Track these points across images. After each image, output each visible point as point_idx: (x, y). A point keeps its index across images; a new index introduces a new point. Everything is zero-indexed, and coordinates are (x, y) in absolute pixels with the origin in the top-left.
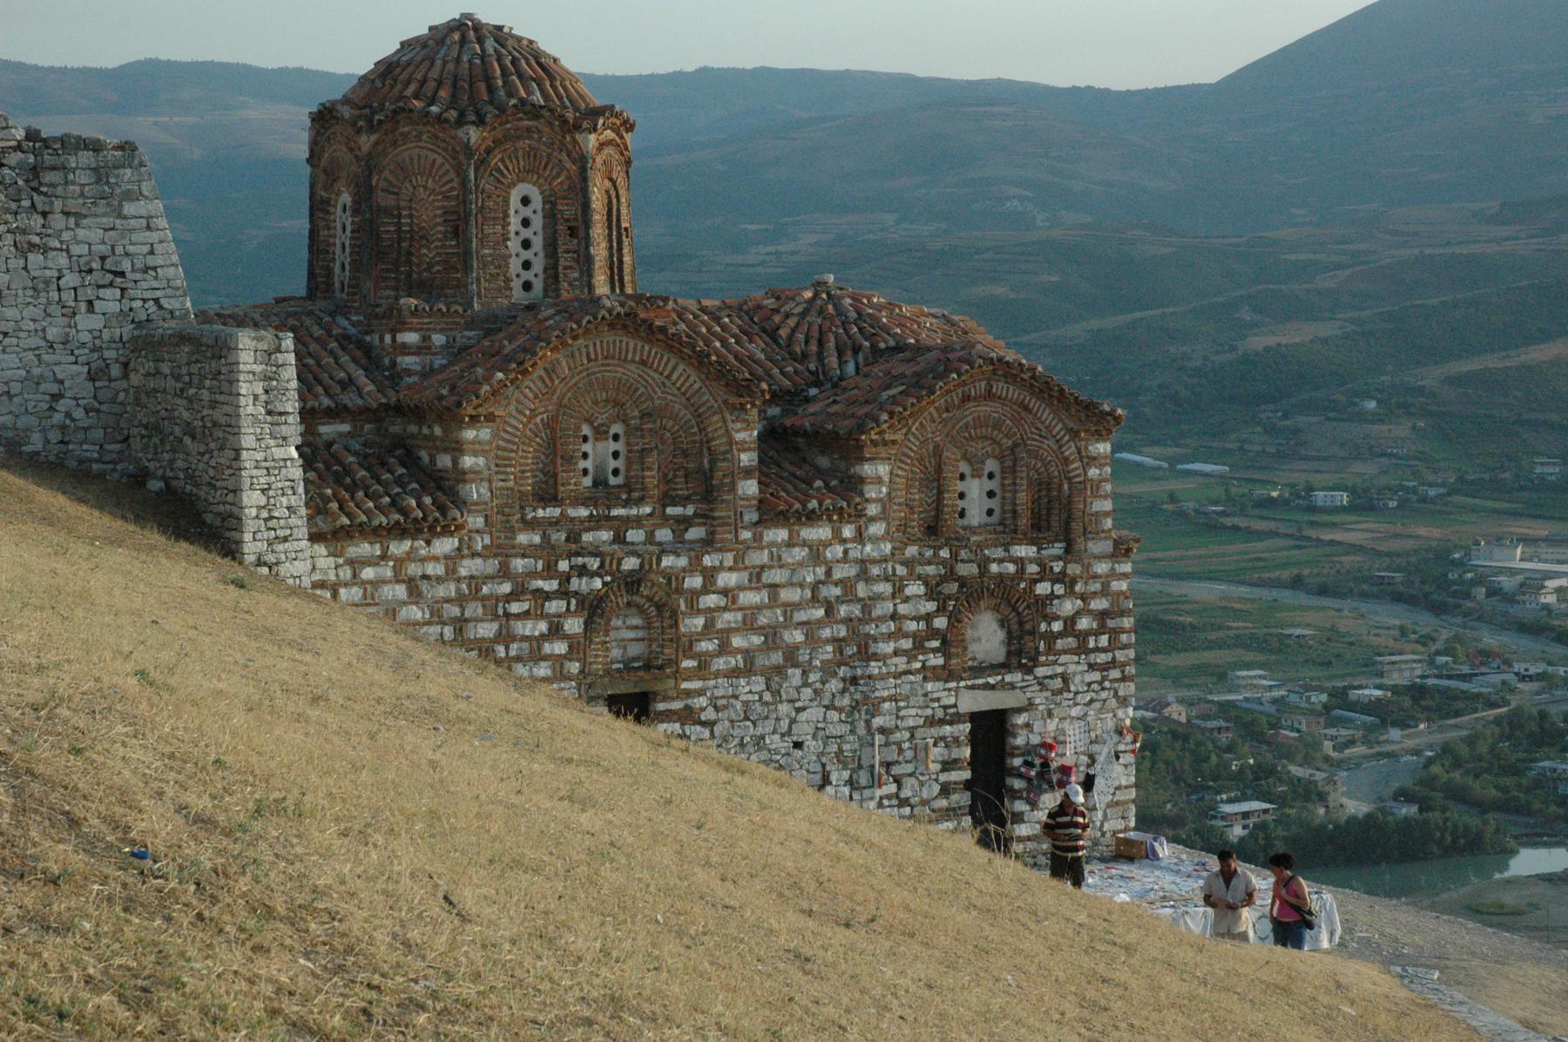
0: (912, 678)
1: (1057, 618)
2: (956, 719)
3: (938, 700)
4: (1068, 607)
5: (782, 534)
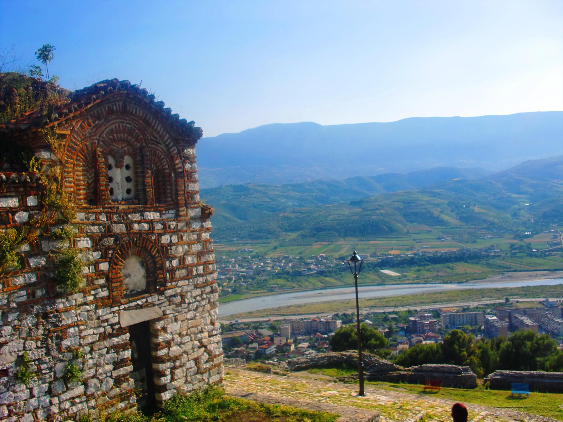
0: (88, 307)
1: (174, 257)
2: (121, 331)
3: (107, 320)
4: (181, 250)
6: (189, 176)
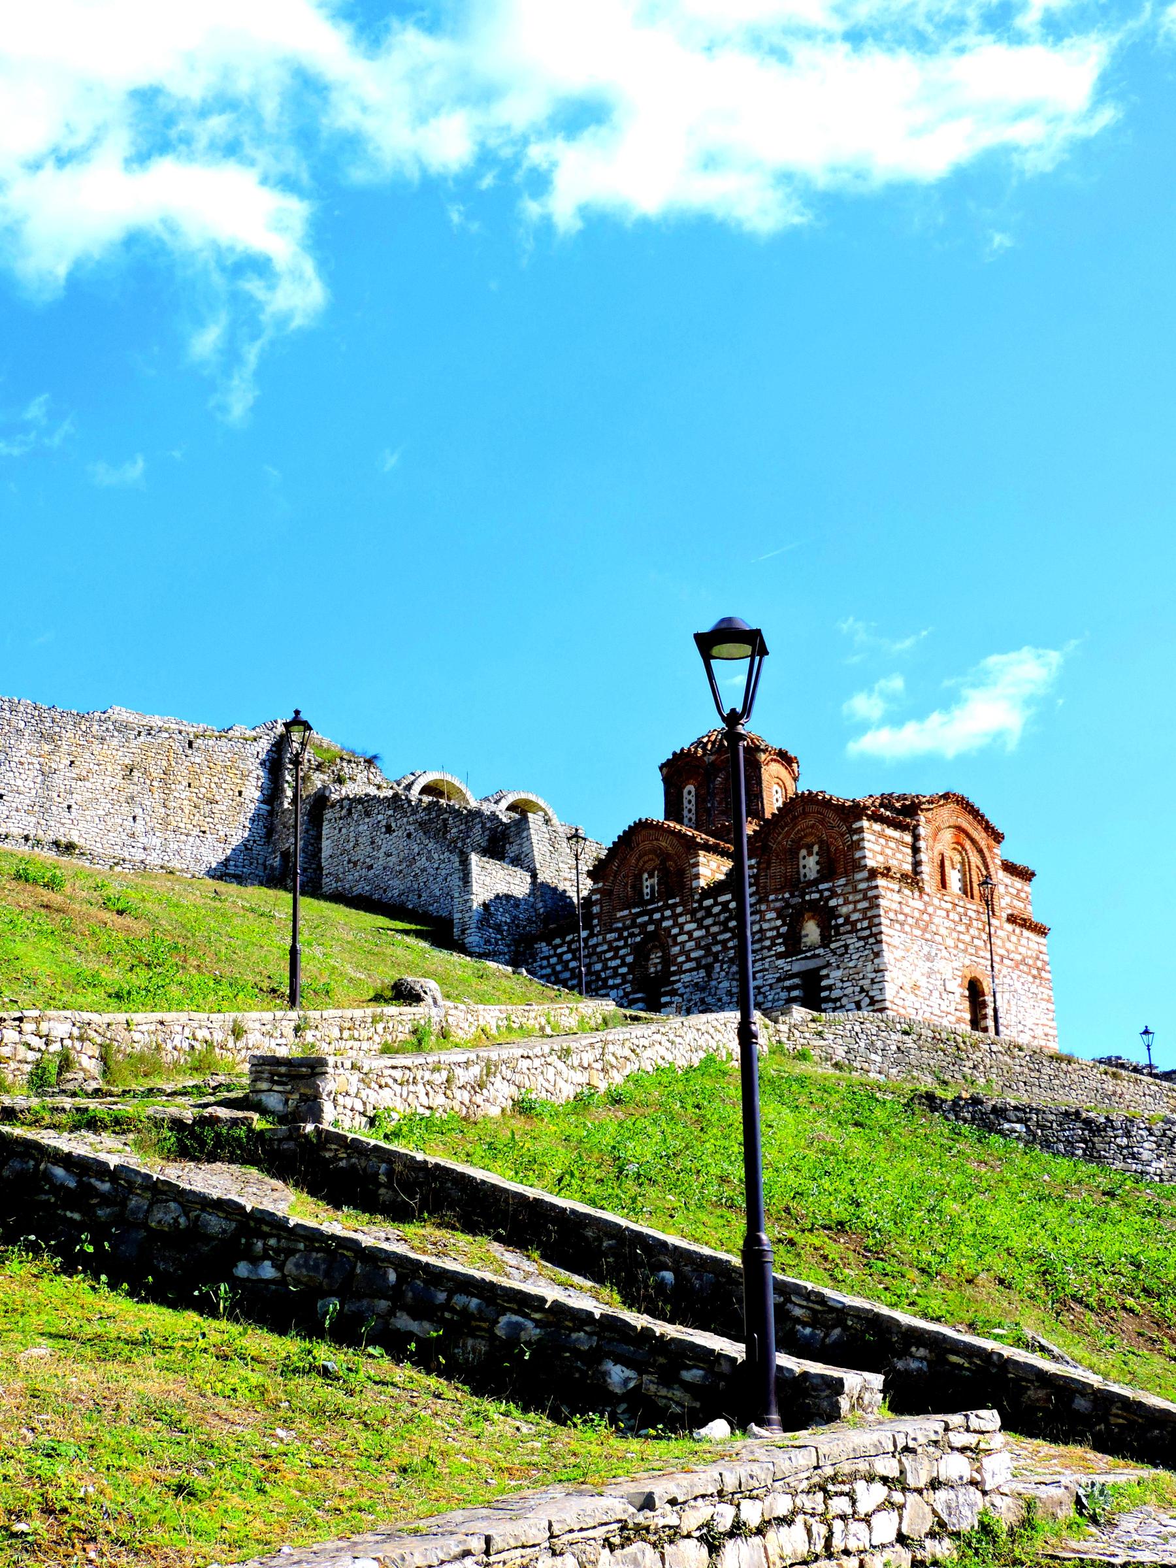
1: (840, 916)
4: (844, 910)
5: (711, 901)
6: (858, 845)
